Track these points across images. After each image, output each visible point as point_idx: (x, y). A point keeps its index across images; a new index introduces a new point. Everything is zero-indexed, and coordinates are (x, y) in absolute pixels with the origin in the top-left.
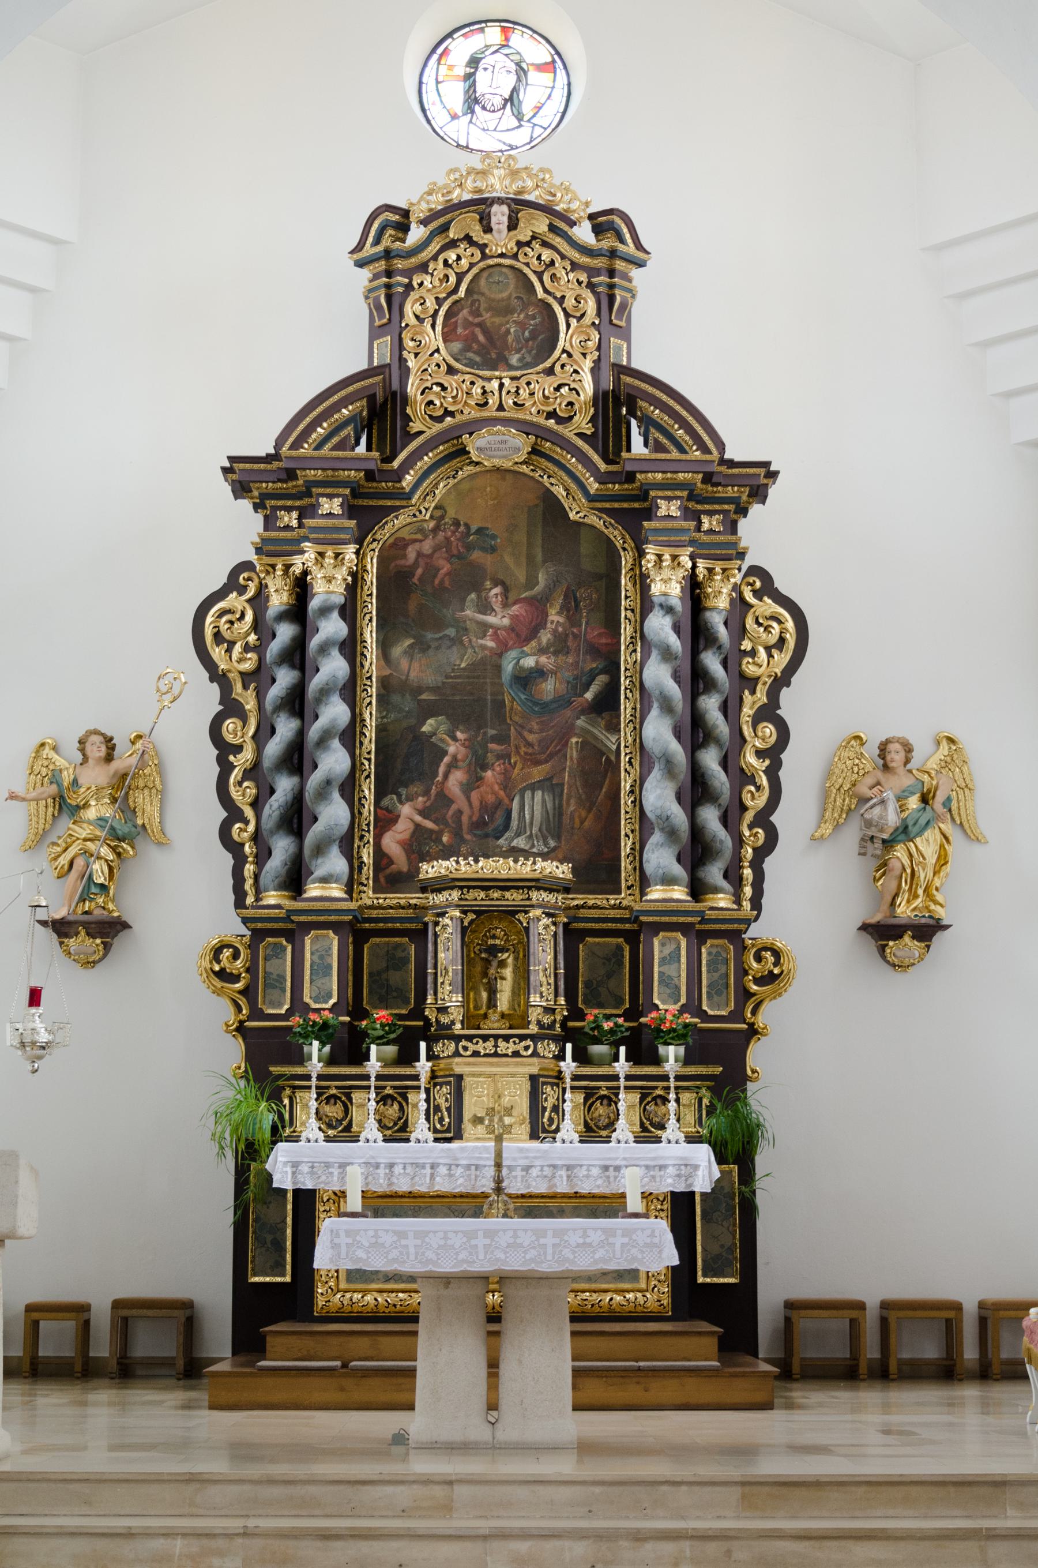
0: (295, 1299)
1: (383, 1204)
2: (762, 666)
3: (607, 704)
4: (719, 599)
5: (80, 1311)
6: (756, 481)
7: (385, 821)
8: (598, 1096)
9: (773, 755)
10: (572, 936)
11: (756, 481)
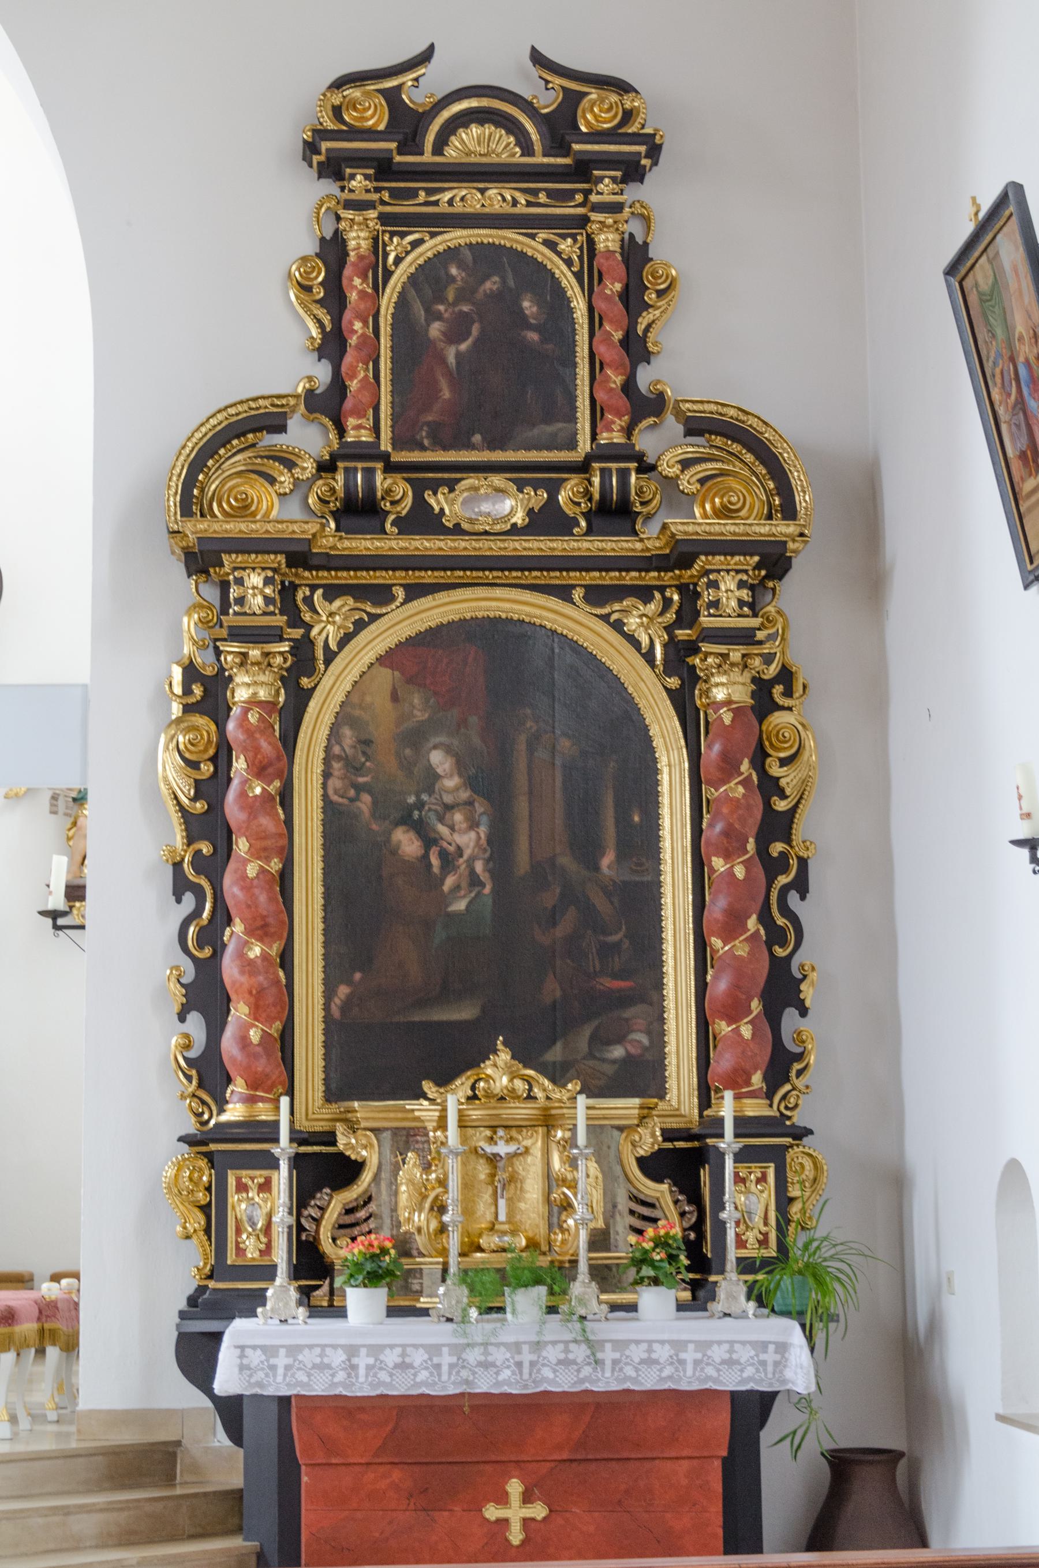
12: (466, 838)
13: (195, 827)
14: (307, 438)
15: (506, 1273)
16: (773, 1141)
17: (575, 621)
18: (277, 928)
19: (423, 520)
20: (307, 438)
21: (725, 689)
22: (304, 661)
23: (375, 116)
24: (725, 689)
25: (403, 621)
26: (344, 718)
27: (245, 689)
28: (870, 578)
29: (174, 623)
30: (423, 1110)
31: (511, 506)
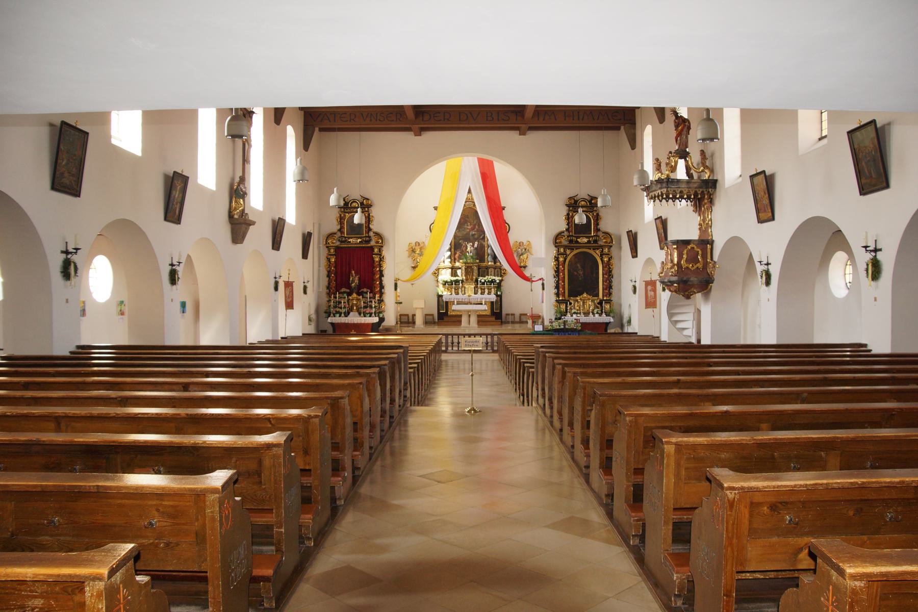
0: (446, 314)
1: (458, 304)
3: (484, 238)
5: (407, 315)
7: (455, 254)
10: (479, 269)
14: (566, 233)
15: (583, 312)
16: (609, 302)
17: (591, 252)
18: (564, 282)
19: (577, 242)
20: (566, 233)
21: (606, 259)
24: (606, 259)
25: (575, 252)
27: (561, 259)
28: (620, 248)
29: (554, 251)
30: (578, 298)
31: (586, 240)
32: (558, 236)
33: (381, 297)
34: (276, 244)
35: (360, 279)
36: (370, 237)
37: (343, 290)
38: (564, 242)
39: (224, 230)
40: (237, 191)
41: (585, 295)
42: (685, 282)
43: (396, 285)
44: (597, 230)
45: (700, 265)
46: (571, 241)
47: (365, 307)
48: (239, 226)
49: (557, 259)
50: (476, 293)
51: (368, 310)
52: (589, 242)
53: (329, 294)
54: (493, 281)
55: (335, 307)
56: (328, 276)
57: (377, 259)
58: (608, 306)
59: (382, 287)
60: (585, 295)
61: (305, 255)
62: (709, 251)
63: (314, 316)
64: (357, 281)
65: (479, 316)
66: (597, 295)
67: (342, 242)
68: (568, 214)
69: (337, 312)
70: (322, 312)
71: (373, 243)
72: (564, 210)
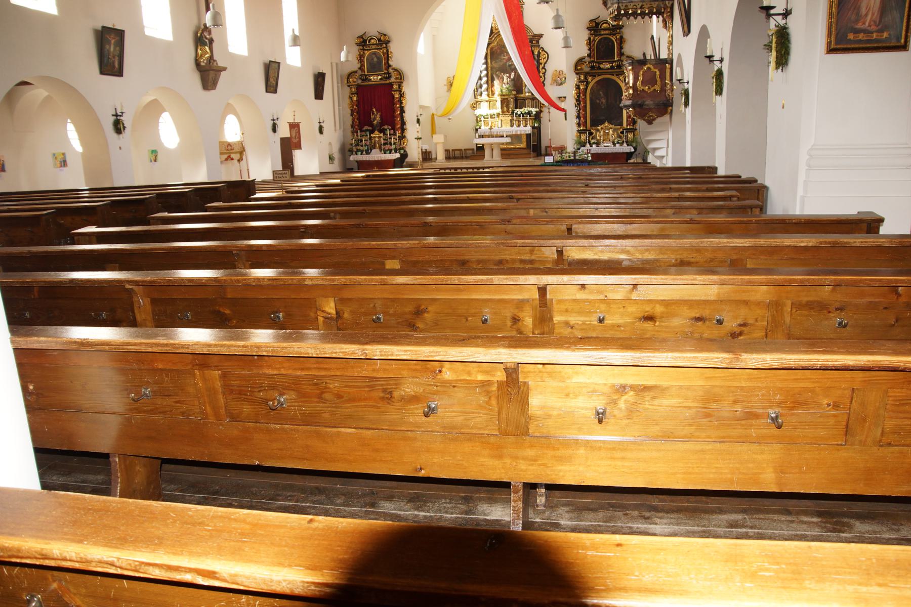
2: (543, 61)
4: (536, 53)
6: (541, 36)
7: (492, 86)
8: (516, 123)
9: (544, 74)
11: (541, 36)
12: (604, 101)
13: (577, 100)
14: (587, 59)
17: (614, 78)
18: (585, 110)
19: (599, 68)
20: (587, 59)
22: (588, 83)
23: (594, 24)
25: (598, 78)
26: (592, 88)
31: (608, 66)
32: (580, 61)
33: (402, 133)
34: (271, 86)
35: (381, 117)
36: (389, 74)
37: (366, 128)
38: (586, 69)
39: (195, 79)
40: (202, 38)
41: (607, 124)
42: (641, 106)
43: (418, 121)
44: (621, 54)
45: (657, 87)
46: (592, 68)
47: (385, 144)
48: (209, 74)
49: (578, 87)
50: (512, 126)
51: (388, 147)
52: (612, 67)
53: (353, 132)
54: (529, 113)
55: (357, 145)
56: (352, 115)
57: (397, 96)
58: (630, 136)
59: (403, 123)
60: (607, 124)
61: (319, 95)
62: (668, 71)
63: (337, 155)
64: (378, 118)
65: (502, 149)
66: (621, 124)
67: (363, 80)
68: (589, 39)
69: (358, 150)
70: (346, 150)
71: (393, 80)
72: (585, 35)
